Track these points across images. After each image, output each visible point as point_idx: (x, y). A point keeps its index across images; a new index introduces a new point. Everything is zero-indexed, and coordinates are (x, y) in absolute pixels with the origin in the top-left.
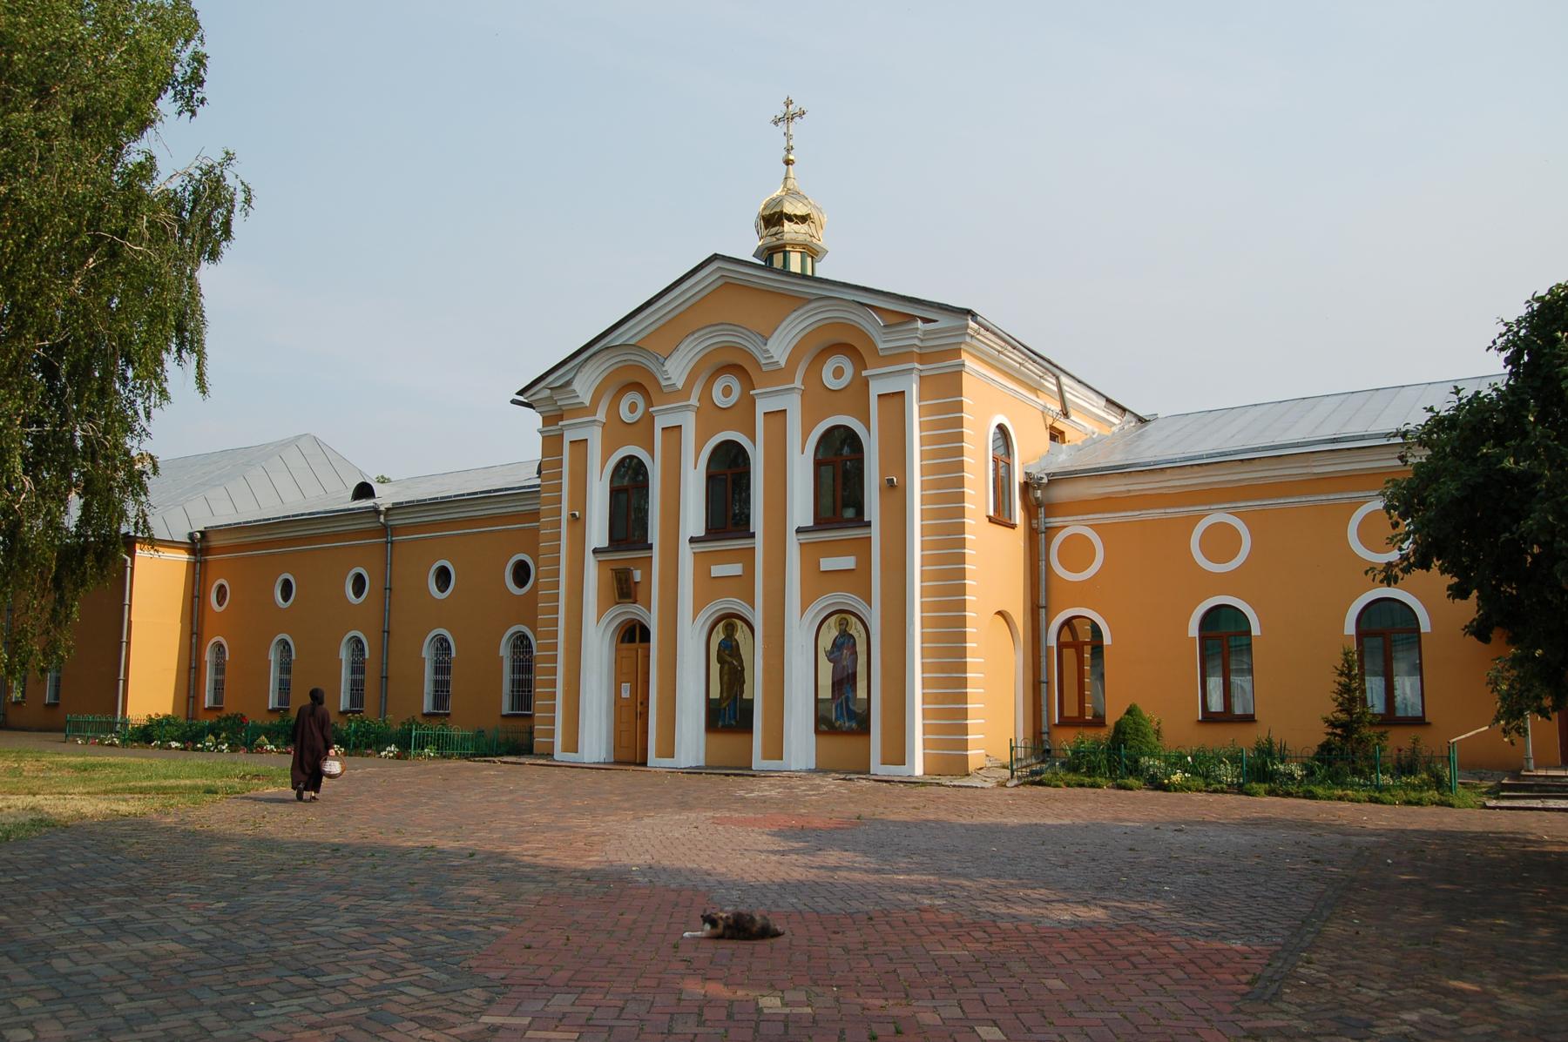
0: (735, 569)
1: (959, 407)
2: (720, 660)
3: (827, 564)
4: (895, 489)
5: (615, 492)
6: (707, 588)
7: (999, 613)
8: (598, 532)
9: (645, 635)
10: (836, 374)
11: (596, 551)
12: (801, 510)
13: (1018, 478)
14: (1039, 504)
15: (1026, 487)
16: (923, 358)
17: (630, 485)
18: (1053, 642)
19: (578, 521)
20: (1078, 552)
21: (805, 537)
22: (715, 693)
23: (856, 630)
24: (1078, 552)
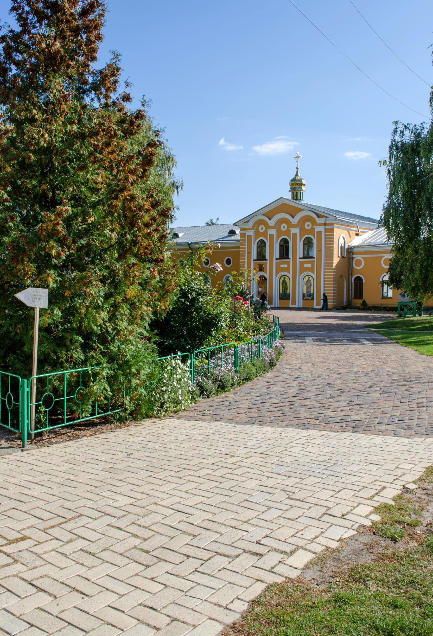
0: (286, 266)
1: (333, 235)
2: (283, 285)
3: (306, 266)
4: (319, 250)
5: (258, 247)
6: (279, 270)
7: (341, 276)
8: (254, 256)
9: (265, 279)
10: (308, 225)
11: (254, 260)
12: (300, 253)
13: (346, 247)
14: (351, 252)
15: (348, 249)
16: (325, 224)
17: (261, 245)
18: (353, 281)
19: (249, 252)
20: (359, 263)
21: (301, 260)
22: (281, 292)
23: (311, 279)
24: (359, 263)
